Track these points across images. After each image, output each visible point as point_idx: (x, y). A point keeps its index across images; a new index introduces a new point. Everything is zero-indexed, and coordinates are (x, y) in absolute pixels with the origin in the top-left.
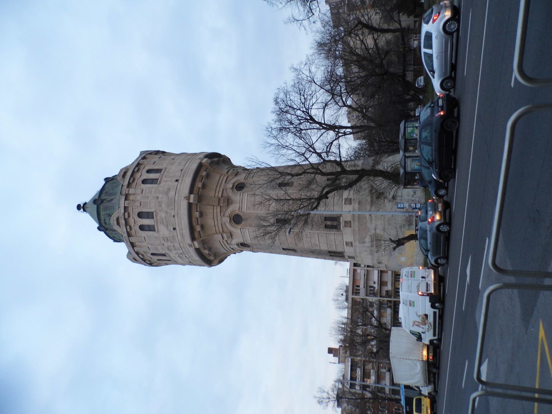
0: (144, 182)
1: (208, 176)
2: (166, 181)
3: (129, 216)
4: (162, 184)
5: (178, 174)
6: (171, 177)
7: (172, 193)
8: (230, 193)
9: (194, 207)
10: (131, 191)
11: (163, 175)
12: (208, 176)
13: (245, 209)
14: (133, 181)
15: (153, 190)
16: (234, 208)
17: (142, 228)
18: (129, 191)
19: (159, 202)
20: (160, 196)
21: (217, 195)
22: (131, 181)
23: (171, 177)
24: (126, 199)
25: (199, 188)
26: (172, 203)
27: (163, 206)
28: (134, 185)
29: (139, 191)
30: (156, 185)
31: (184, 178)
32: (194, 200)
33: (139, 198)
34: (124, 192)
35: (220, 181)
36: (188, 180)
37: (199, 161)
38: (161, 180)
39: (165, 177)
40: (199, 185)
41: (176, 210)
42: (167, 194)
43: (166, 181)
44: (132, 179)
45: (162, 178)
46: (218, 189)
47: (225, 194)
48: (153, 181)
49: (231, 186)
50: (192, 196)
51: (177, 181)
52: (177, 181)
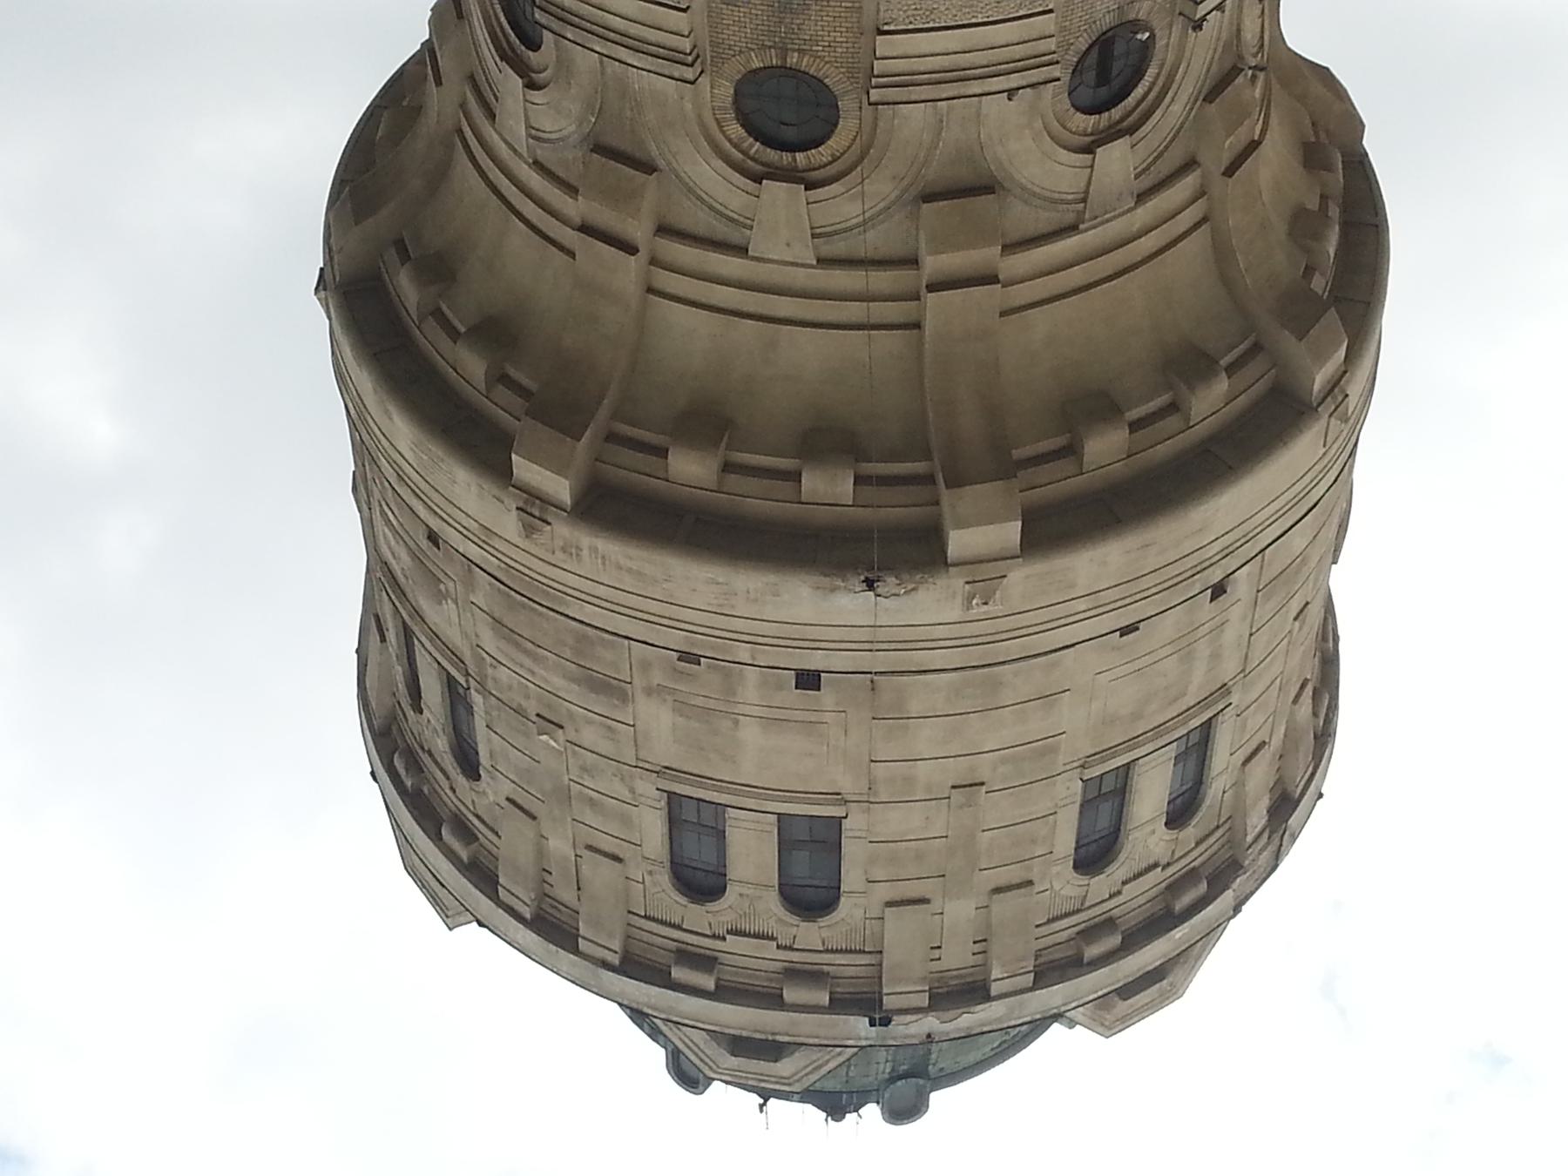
0: (810, 897)
28: (848, 966)
37: (562, 530)
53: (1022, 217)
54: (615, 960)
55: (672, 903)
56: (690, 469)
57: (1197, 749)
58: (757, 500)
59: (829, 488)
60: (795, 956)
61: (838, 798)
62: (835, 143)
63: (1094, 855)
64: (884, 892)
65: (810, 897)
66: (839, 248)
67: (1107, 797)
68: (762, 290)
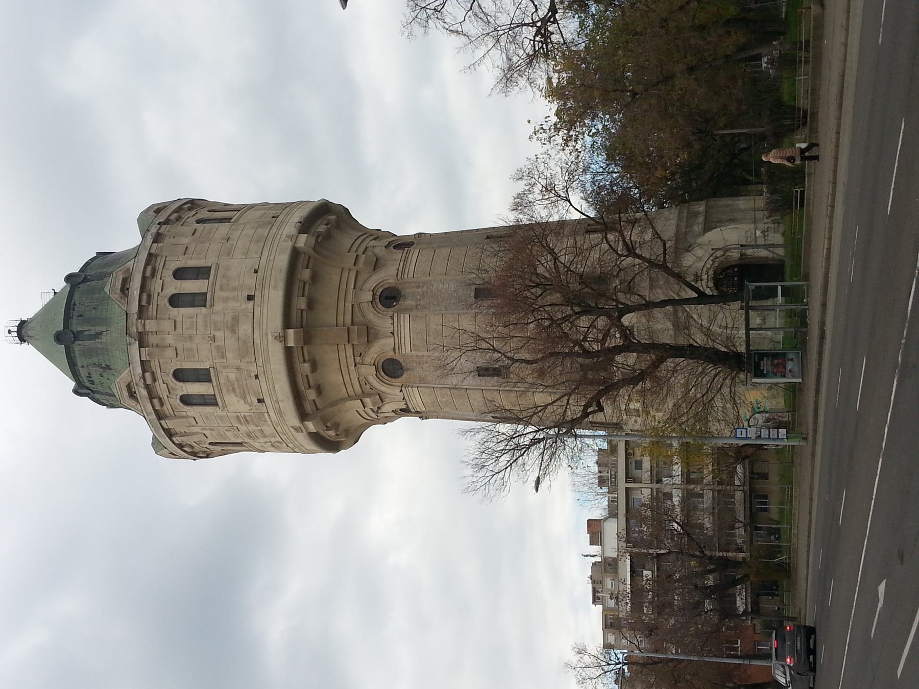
0: (176, 301)
1: (315, 278)
2: (226, 300)
3: (154, 380)
4: (218, 307)
5: (250, 281)
6: (235, 289)
7: (245, 328)
8: (371, 316)
9: (297, 355)
10: (151, 325)
11: (214, 284)
12: (315, 278)
13: (407, 350)
14: (149, 302)
15: (200, 321)
16: (382, 348)
17: (186, 400)
18: (144, 326)
19: (218, 347)
20: (219, 334)
21: (341, 319)
22: (144, 303)
23: (235, 289)
24: (141, 346)
25: (302, 310)
26: (247, 349)
27: (229, 355)
28: (152, 309)
29: (167, 325)
30: (204, 310)
31: (266, 292)
32: (296, 341)
33: (170, 340)
34: (134, 330)
35: (343, 286)
36: (275, 297)
37: (290, 244)
38: (213, 298)
39: (221, 289)
40: (301, 303)
41: (260, 363)
42: (233, 331)
43: (226, 300)
44: (145, 296)
45: (213, 292)
46: (341, 305)
47: (358, 317)
48: (198, 300)
49: (369, 296)
50: (291, 332)
51: (250, 298)
52: (250, 298)
53: (361, 349)
54: (153, 251)
55: (173, 265)
56: (306, 274)
57: (209, 401)
58: (296, 289)
59: (301, 303)
60: (156, 296)
61: (212, 305)
62: (380, 306)
63: (180, 375)
64: (179, 319)
65: (176, 301)
66: (356, 309)
67: (203, 376)
68: (346, 293)
